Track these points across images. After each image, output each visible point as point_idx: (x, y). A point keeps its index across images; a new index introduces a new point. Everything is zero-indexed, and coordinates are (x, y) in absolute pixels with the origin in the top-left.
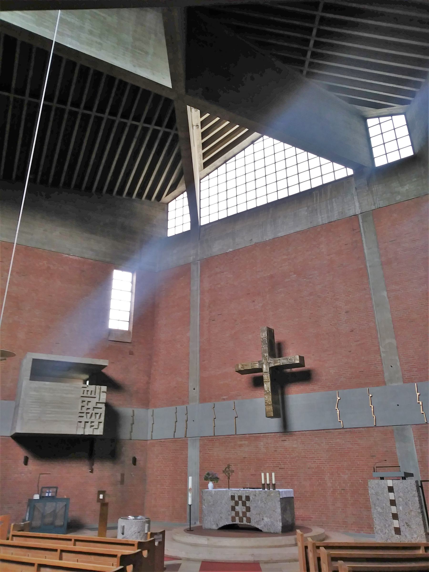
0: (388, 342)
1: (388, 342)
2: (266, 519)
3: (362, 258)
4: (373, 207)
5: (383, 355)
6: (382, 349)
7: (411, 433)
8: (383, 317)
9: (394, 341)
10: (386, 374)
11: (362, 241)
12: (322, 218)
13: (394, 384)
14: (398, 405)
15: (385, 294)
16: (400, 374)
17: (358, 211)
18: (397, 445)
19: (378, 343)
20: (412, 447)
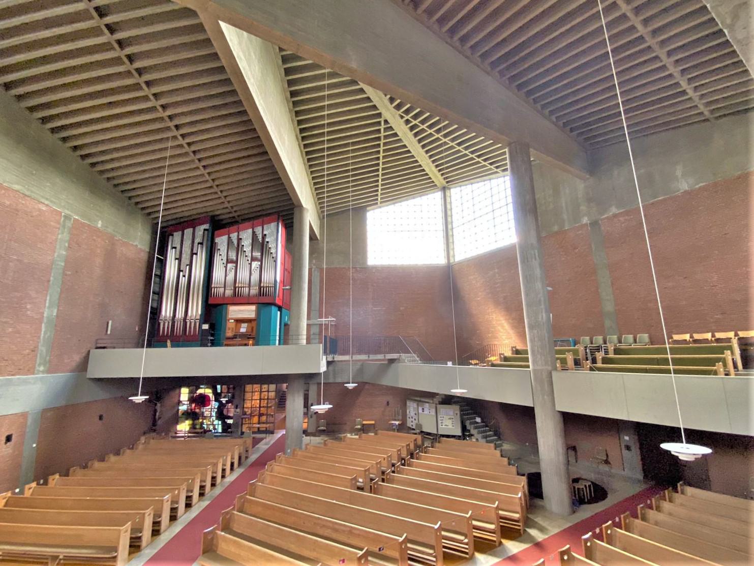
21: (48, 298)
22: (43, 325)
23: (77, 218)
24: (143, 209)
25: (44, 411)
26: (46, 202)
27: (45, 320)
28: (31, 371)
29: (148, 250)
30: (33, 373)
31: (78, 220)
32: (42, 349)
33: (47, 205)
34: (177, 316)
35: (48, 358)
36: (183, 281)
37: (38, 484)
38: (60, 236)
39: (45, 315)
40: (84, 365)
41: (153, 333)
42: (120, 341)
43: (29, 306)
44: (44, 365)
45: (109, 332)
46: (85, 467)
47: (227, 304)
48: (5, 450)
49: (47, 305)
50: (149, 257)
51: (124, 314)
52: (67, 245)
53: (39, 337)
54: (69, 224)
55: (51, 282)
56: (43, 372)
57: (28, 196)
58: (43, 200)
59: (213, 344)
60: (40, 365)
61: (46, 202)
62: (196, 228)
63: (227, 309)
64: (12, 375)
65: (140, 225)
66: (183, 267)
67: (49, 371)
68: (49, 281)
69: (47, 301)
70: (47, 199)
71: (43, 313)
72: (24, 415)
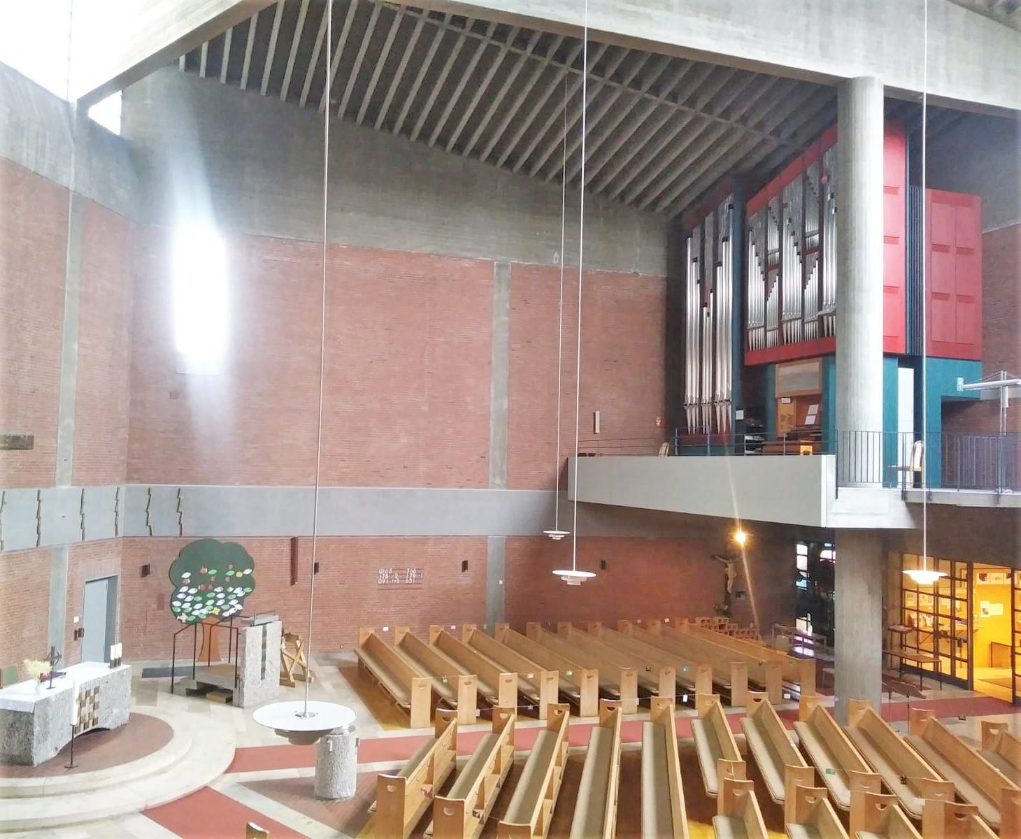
0: (67, 423)
1: (67, 423)
2: (115, 711)
3: (61, 271)
4: (87, 195)
5: (59, 441)
6: (60, 433)
7: (66, 555)
8: (69, 383)
9: (73, 424)
10: (58, 471)
11: (67, 242)
12: (28, 154)
13: (64, 487)
14: (63, 517)
15: (76, 346)
16: (71, 472)
17: (72, 188)
18: (52, 573)
19: (58, 422)
20: (65, 574)
21: (492, 387)
22: (491, 422)
23: (516, 261)
24: (638, 200)
25: (510, 539)
26: (469, 254)
27: (493, 416)
28: (483, 483)
29: (662, 275)
30: (487, 487)
31: (518, 265)
32: (495, 454)
33: (471, 259)
34: (691, 393)
35: (504, 468)
36: (708, 322)
37: (480, 628)
38: (495, 297)
39: (492, 409)
40: (564, 479)
41: (680, 433)
42: (627, 443)
43: (469, 399)
44: (502, 478)
45: (597, 431)
46: (554, 630)
47: (776, 363)
48: (465, 579)
49: (492, 396)
50: (668, 288)
51: (630, 399)
52: (508, 306)
53: (488, 439)
54: (506, 274)
55: (493, 364)
56: (500, 486)
57: (445, 256)
58: (464, 254)
59: (757, 448)
60: (494, 475)
61: (469, 254)
62: (720, 208)
63: (774, 371)
64: (461, 487)
65: (638, 233)
66: (709, 301)
67: (508, 486)
68: (490, 363)
69: (492, 391)
70: (469, 250)
71: (489, 407)
72: (482, 540)
